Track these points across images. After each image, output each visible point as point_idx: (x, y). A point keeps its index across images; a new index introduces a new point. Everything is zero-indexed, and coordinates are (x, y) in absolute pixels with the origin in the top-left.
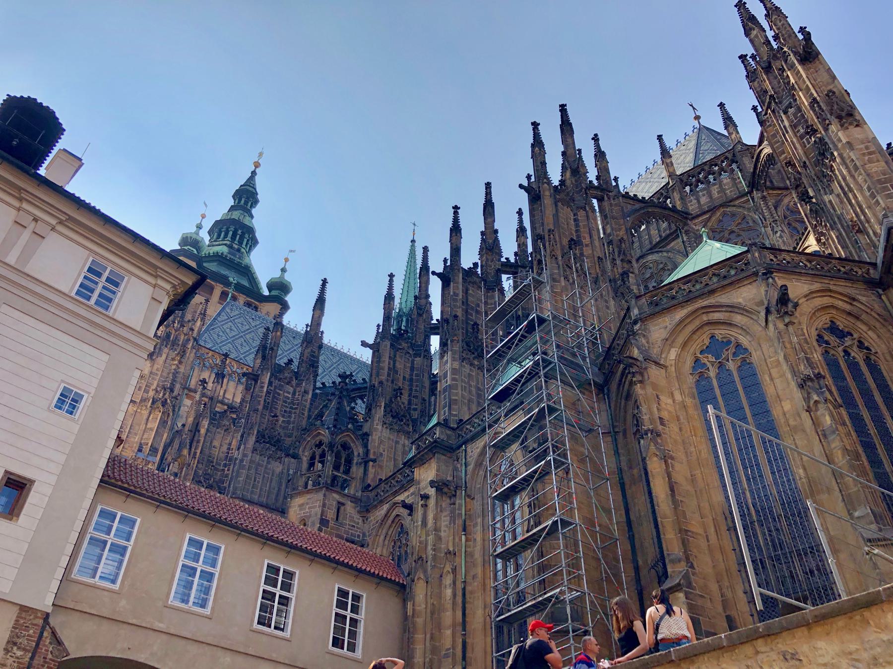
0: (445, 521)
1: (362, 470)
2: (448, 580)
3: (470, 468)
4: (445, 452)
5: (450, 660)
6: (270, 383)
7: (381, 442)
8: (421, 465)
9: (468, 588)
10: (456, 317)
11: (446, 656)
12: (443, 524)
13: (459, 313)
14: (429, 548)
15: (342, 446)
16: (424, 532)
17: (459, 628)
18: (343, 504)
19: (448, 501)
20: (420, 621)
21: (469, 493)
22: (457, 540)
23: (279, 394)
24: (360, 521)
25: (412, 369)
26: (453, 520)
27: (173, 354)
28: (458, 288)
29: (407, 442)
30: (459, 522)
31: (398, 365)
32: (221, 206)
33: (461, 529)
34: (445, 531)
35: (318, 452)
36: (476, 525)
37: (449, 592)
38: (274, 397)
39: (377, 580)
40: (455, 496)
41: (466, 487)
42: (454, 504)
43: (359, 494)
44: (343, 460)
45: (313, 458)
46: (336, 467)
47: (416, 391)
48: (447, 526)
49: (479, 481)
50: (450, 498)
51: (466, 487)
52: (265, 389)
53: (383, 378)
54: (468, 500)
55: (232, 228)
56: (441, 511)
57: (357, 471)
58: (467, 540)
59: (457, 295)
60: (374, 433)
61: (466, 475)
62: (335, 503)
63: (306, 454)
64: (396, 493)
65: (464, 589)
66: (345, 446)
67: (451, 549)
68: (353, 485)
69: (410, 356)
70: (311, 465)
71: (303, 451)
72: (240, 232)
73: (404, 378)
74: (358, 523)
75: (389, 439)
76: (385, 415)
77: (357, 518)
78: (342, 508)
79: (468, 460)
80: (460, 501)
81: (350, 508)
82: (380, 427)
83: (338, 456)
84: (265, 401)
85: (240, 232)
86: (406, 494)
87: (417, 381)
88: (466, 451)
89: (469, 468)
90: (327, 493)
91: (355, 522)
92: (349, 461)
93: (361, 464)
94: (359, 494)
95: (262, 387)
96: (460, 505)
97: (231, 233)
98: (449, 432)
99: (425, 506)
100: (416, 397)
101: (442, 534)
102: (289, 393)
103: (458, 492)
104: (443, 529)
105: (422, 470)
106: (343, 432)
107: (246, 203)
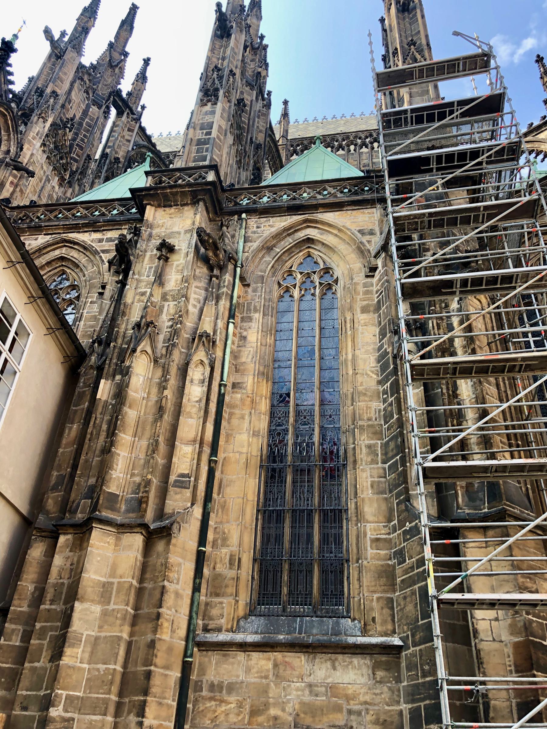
0: (196, 293)
2: (196, 373)
4: (210, 209)
5: (188, 493)
8: (159, 206)
9: (227, 398)
11: (180, 485)
17: (207, 450)
19: (205, 270)
20: (131, 414)
25: (85, 113)
29: (57, 187)
34: (195, 306)
36: (250, 319)
37: (195, 391)
39: (52, 321)
47: (82, 140)
49: (262, 267)
50: (211, 268)
64: (76, 228)
65: (221, 398)
69: (88, 98)
75: (42, 167)
76: (47, 136)
82: (38, 144)
86: (98, 236)
87: (87, 131)
89: (249, 244)
100: (81, 148)
101: (190, 308)
103: (230, 267)
104: (192, 301)
105: (161, 212)
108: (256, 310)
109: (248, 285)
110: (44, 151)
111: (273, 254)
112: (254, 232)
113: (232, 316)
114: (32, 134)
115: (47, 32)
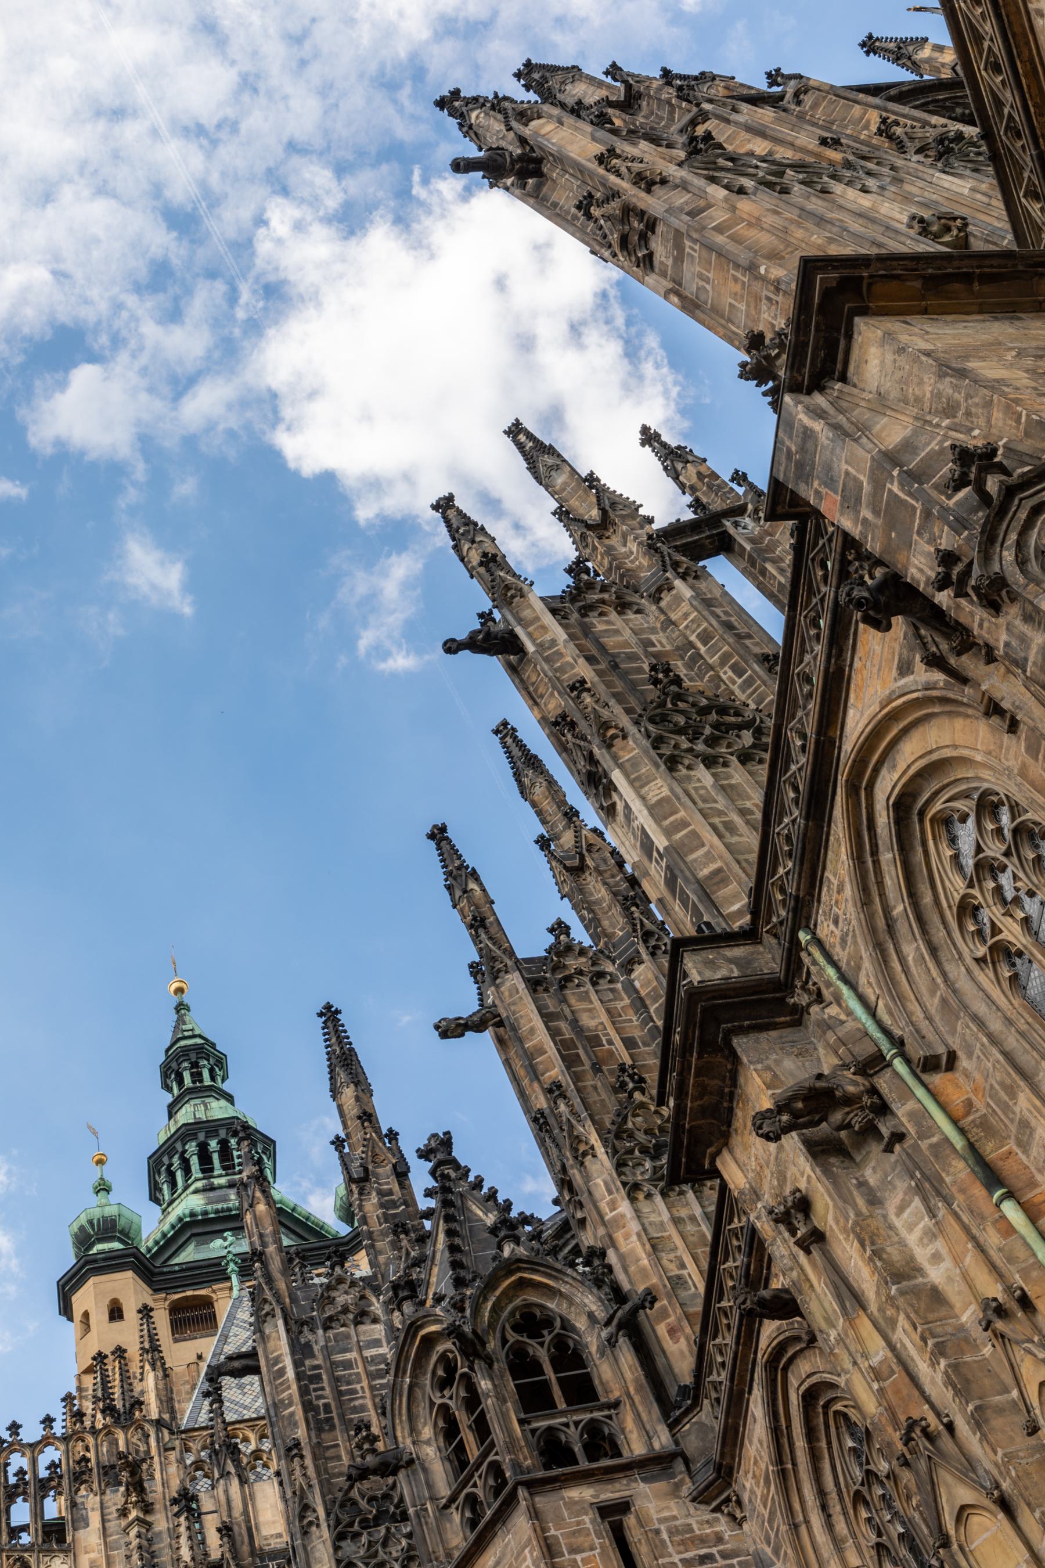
1: (627, 1357)
3: (867, 976)
6: (301, 1351)
7: (655, 1246)
10: (579, 686)
12: (912, 1239)
13: (584, 670)
14: (922, 1367)
15: (516, 1328)
16: (866, 1327)
18: (624, 1507)
19: (875, 1149)
21: (917, 1052)
22: (992, 1239)
23: (348, 1365)
24: (723, 1526)
26: (930, 1188)
27: (116, 1498)
28: (544, 628)
30: (958, 1172)
31: (588, 1021)
32: (148, 1118)
33: (978, 1191)
34: (936, 1258)
35: (453, 1399)
38: (336, 1380)
40: (883, 1109)
41: (899, 1043)
42: (899, 1137)
43: (663, 1439)
44: (547, 1367)
45: (450, 1431)
46: (534, 1399)
48: (930, 1235)
51: (899, 1043)
52: (290, 1373)
53: (556, 1071)
54: (936, 1079)
55: (192, 1147)
56: (874, 1201)
57: (616, 1372)
58: (1032, 1214)
59: (553, 642)
60: (619, 1236)
61: (872, 1013)
62: (588, 1520)
63: (427, 1432)
66: (532, 1322)
67: (995, 1290)
68: (630, 1423)
70: (458, 1459)
71: (413, 1430)
72: (213, 1144)
73: (630, 1043)
74: (719, 1539)
76: (620, 1166)
77: (699, 1520)
78: (630, 1521)
79: (841, 954)
80: (911, 1101)
81: (656, 1505)
83: (522, 1365)
84: (308, 1407)
85: (213, 1144)
88: (819, 943)
89: (862, 980)
90: (540, 1501)
91: (703, 1541)
92: (569, 1355)
93: (612, 1342)
94: (663, 1439)
95: (282, 1372)
96: (921, 1116)
97: (194, 1161)
98: (738, 952)
99: (815, 1240)
101: (936, 1275)
102: (377, 1343)
103: (883, 1083)
104: (922, 1255)
106: (490, 1285)
107: (197, 1077)
108: (1011, 1091)
109: (952, 1056)
110: (649, 1196)
111: (902, 928)
112: (843, 941)
113: (991, 1176)
114: (604, 1206)
115: (451, 1029)
